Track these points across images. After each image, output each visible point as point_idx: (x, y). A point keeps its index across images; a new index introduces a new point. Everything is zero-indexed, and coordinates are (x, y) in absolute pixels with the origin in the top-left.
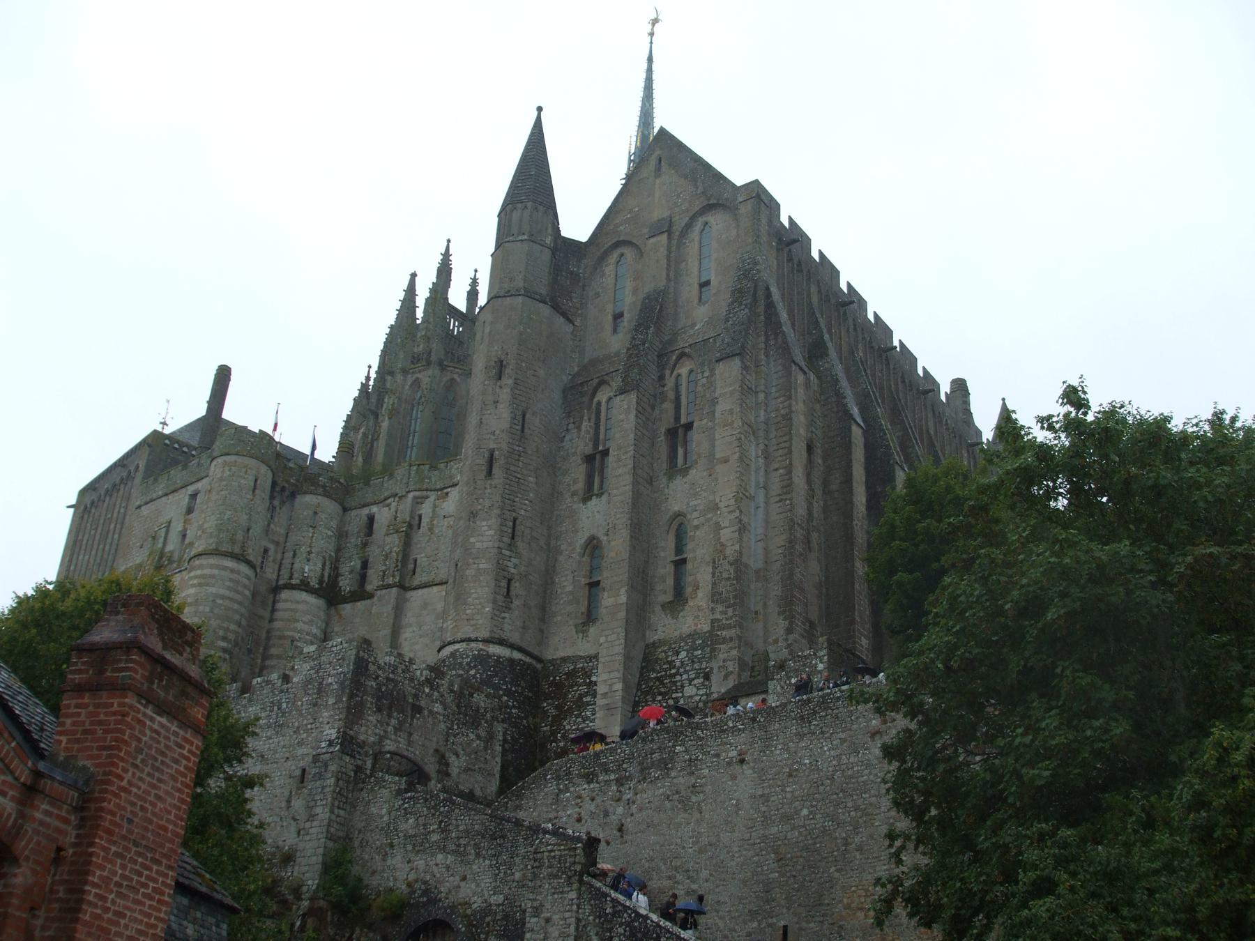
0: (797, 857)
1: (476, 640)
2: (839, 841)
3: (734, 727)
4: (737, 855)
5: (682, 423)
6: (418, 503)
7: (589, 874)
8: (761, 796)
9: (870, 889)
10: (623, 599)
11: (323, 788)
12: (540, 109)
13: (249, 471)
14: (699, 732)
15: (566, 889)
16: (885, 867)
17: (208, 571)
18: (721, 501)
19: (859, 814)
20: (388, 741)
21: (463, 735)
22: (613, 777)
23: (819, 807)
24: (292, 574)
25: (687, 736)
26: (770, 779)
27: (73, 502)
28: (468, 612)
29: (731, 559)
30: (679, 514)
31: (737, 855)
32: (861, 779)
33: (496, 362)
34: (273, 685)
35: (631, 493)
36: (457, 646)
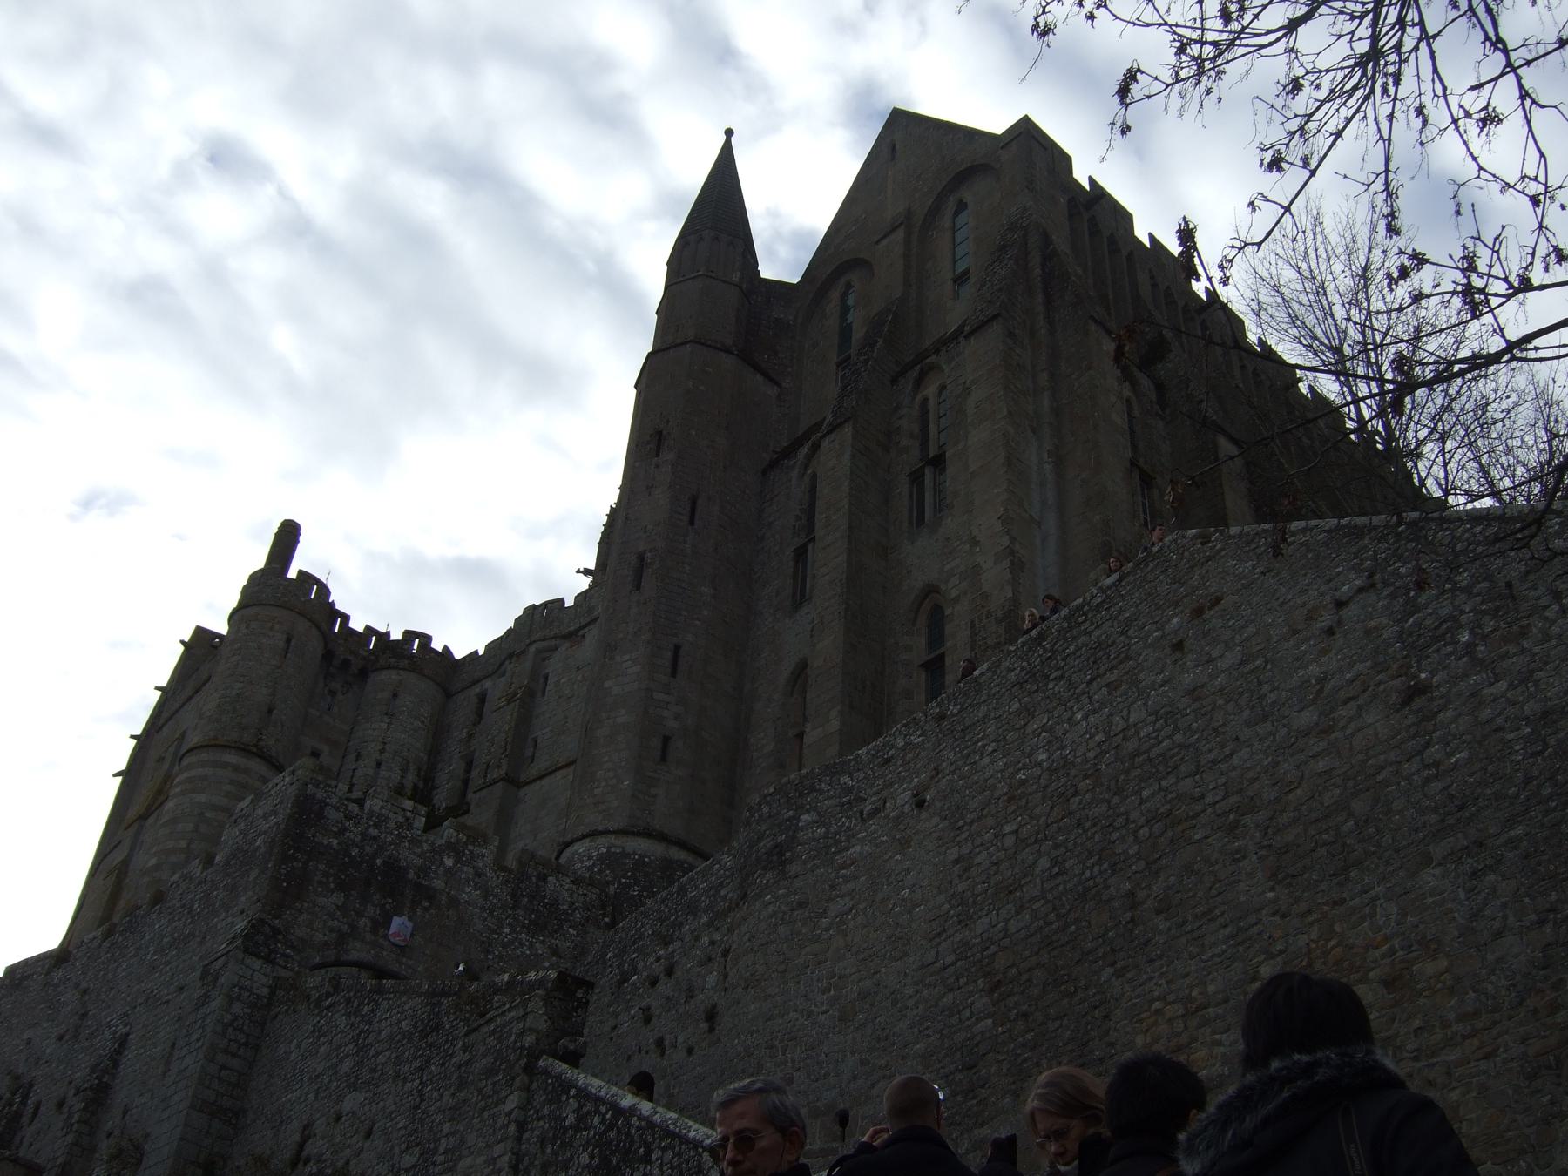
0: (1029, 970)
1: (606, 832)
2: (1117, 904)
3: (903, 749)
4: (911, 1003)
5: (931, 455)
6: (544, 660)
7: (555, 1055)
8: (957, 861)
9: (1194, 994)
10: (835, 725)
11: (204, 1019)
12: (729, 133)
13: (277, 627)
14: (845, 779)
15: (503, 1093)
16: (1228, 931)
17: (193, 773)
18: (980, 531)
19: (1157, 828)
20: (358, 945)
21: (522, 944)
22: (704, 919)
23: (1070, 846)
24: (352, 785)
25: (821, 792)
26: (972, 822)
27: (122, 765)
28: (597, 791)
29: (1000, 614)
30: (930, 590)
31: (911, 1003)
32: (1156, 751)
33: (651, 436)
34: (191, 879)
35: (845, 565)
36: (576, 847)
